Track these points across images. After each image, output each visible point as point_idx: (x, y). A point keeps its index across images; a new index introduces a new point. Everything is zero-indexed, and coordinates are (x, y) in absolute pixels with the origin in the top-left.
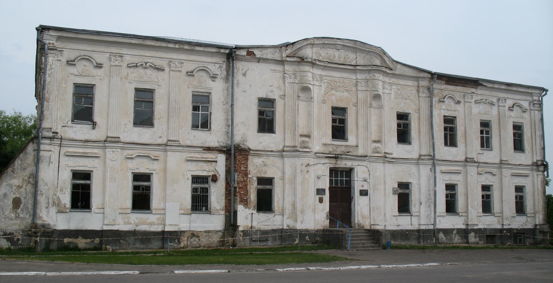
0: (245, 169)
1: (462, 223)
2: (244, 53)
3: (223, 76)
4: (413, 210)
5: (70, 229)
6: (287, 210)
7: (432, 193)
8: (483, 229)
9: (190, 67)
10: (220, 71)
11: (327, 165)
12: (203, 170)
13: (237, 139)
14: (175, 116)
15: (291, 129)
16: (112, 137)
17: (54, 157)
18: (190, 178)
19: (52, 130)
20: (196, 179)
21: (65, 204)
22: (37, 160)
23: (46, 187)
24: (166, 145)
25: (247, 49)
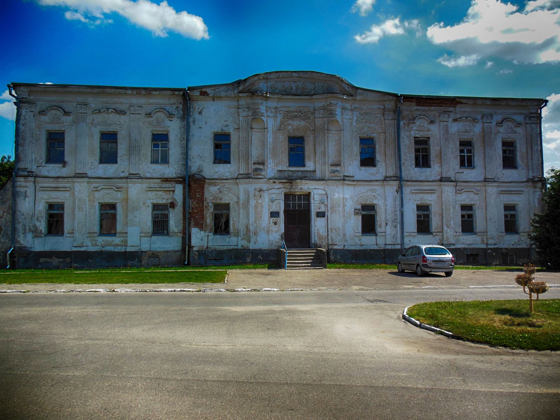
0: (200, 196)
2: (197, 93)
3: (180, 115)
4: (378, 230)
5: (45, 250)
6: (241, 232)
7: (398, 213)
8: (462, 249)
9: (149, 109)
10: (177, 111)
11: (281, 190)
12: (162, 198)
13: (194, 169)
14: (135, 154)
15: (245, 159)
16: (79, 174)
17: (30, 191)
18: (151, 206)
19: (28, 170)
20: (156, 207)
21: (41, 230)
22: (15, 195)
23: (23, 217)
24: (127, 178)
25: (200, 90)
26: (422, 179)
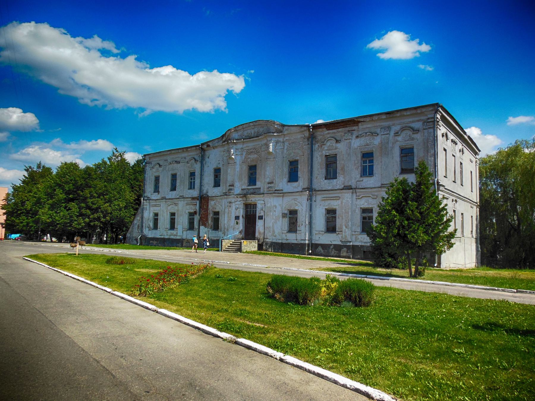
1: (339, 240)
17: (148, 207)
26: (330, 188)
